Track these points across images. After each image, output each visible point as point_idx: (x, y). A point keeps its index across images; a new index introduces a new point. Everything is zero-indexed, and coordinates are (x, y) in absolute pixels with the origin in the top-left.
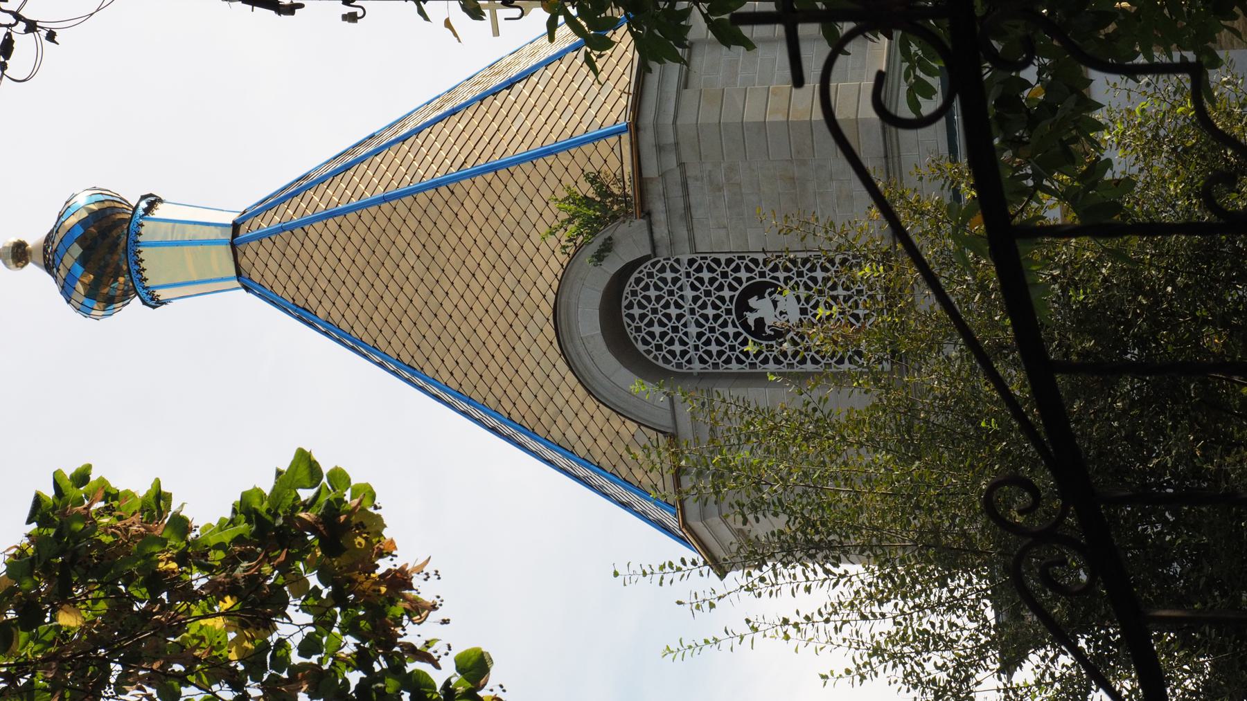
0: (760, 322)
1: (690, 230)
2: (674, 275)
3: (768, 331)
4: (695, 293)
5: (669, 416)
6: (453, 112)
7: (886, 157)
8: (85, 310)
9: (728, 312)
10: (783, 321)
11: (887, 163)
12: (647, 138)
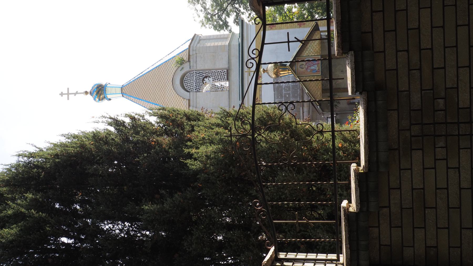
8: (95, 99)
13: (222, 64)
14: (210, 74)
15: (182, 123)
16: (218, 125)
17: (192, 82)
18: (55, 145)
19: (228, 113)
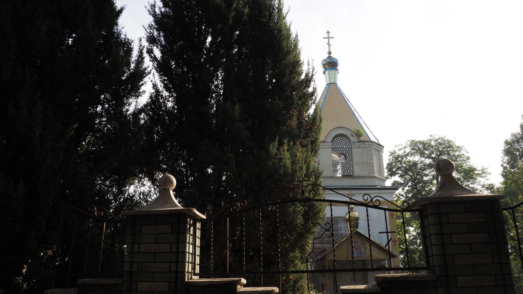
8: (324, 60)
13: (357, 171)
15: (309, 137)
16: (308, 169)
17: (341, 144)
18: (289, 29)
19: (319, 177)
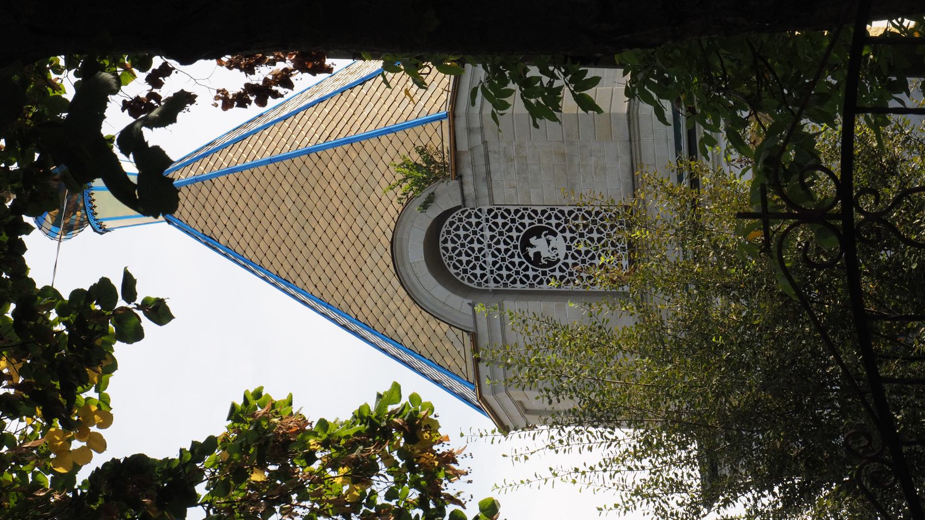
0: (538, 255)
1: (490, 189)
2: (477, 220)
3: (543, 261)
4: (492, 233)
5: (472, 320)
6: (321, 100)
7: (630, 140)
9: (515, 247)
10: (554, 254)
11: (631, 144)
12: (461, 124)
14: (553, 221)
